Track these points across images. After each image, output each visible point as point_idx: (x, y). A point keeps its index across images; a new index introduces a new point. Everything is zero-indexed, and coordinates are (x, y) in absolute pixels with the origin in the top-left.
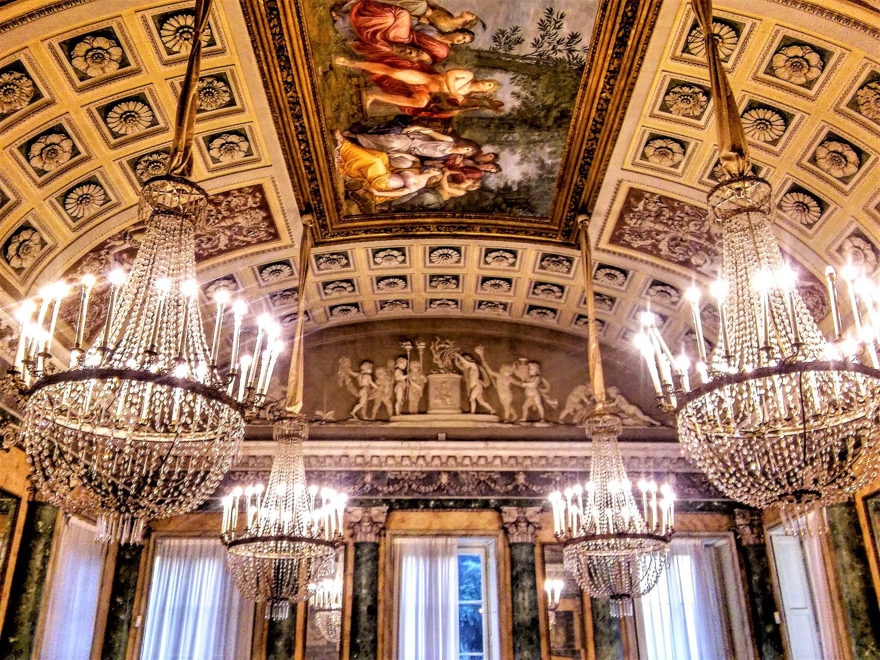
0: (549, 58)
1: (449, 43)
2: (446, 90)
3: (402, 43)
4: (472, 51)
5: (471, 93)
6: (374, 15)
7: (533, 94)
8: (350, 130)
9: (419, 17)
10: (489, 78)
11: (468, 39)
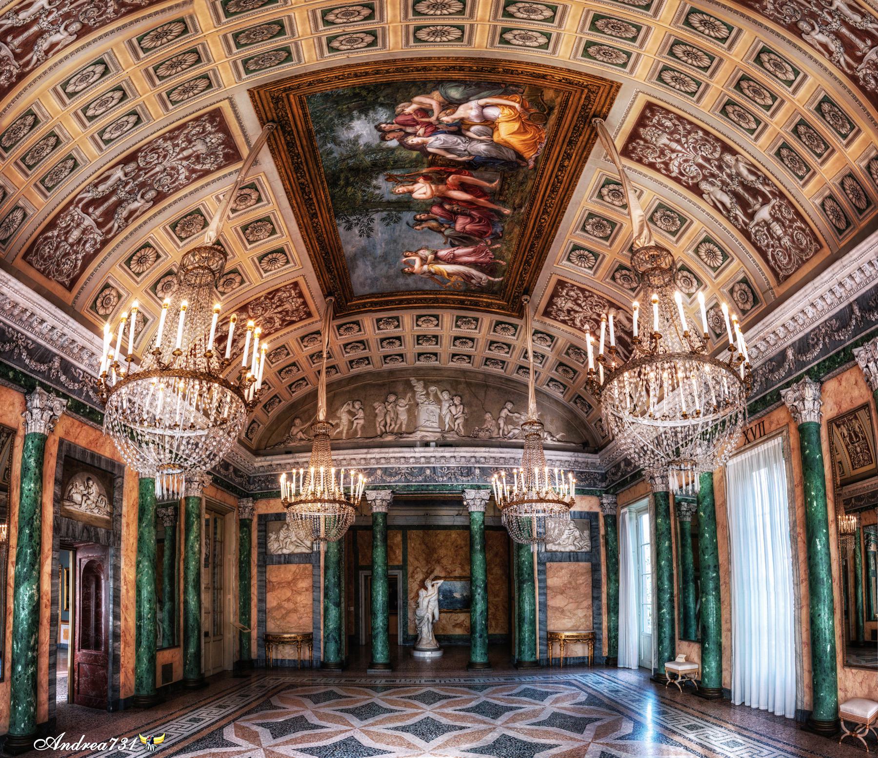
6: (477, 231)
8: (519, 166)
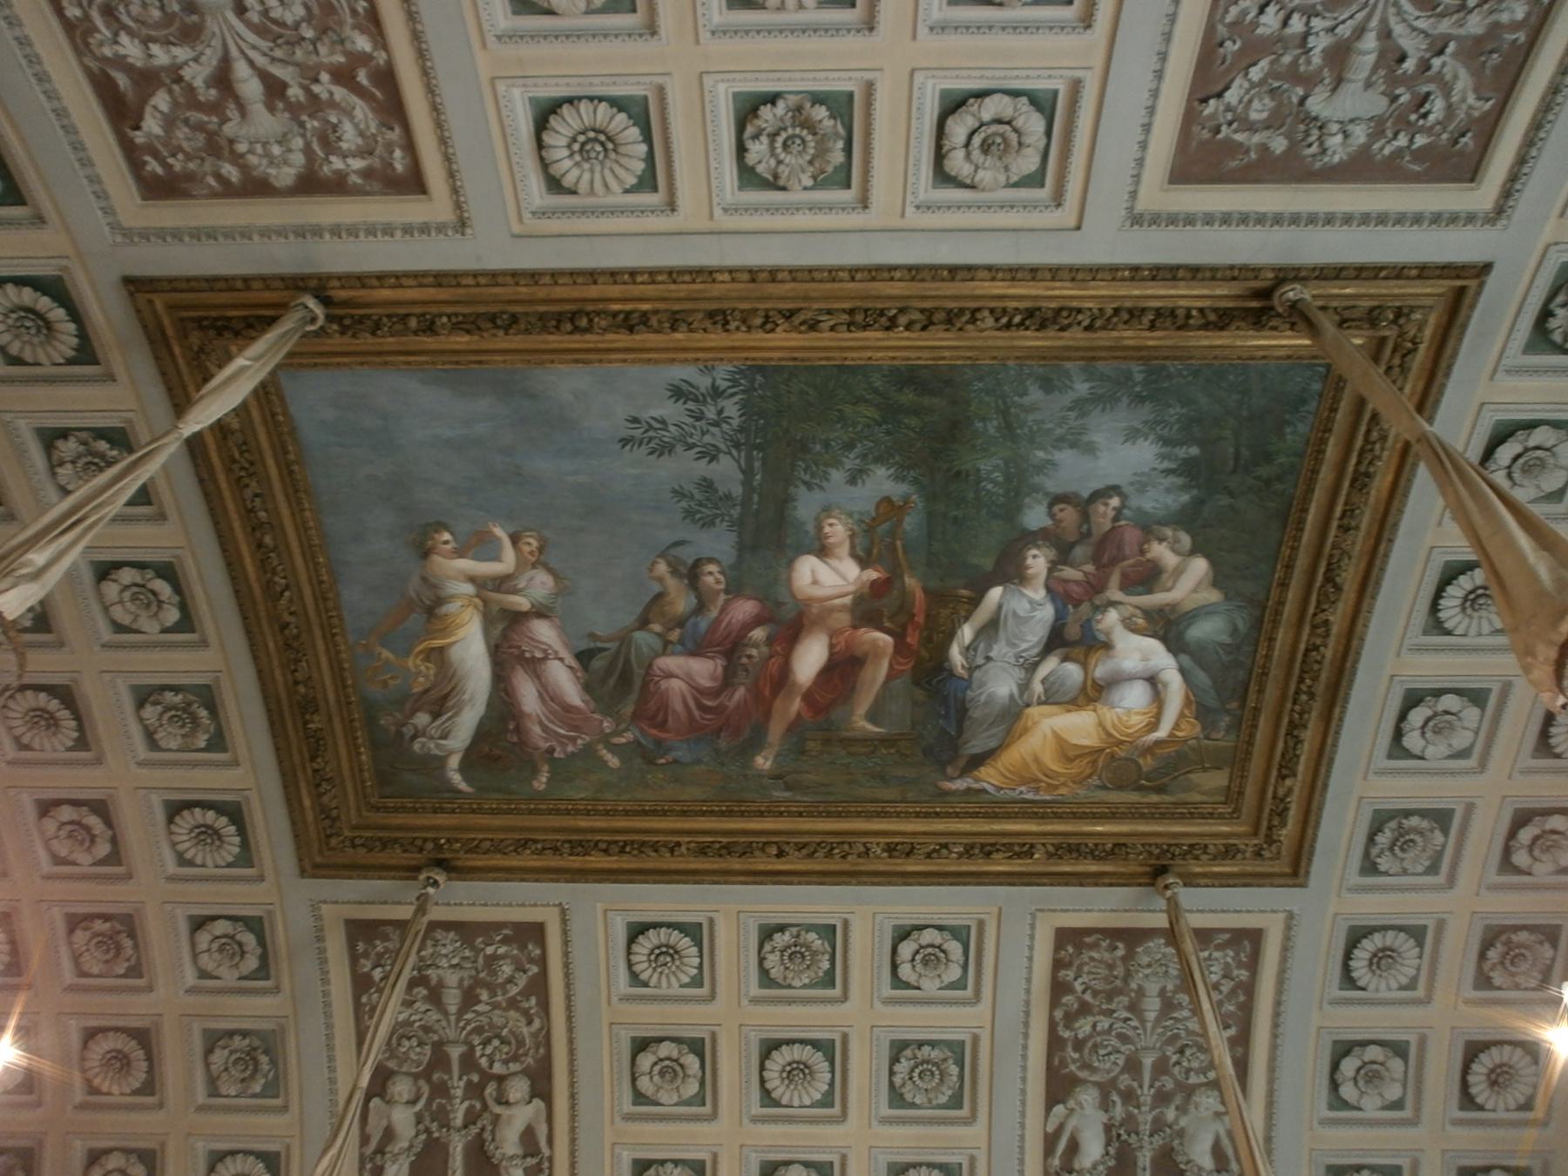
0: (741, 430)
1: (722, 597)
2: (848, 600)
3: (726, 669)
5: (854, 555)
6: (664, 706)
7: (850, 446)
8: (942, 765)
9: (667, 643)
10: (810, 528)
11: (712, 568)
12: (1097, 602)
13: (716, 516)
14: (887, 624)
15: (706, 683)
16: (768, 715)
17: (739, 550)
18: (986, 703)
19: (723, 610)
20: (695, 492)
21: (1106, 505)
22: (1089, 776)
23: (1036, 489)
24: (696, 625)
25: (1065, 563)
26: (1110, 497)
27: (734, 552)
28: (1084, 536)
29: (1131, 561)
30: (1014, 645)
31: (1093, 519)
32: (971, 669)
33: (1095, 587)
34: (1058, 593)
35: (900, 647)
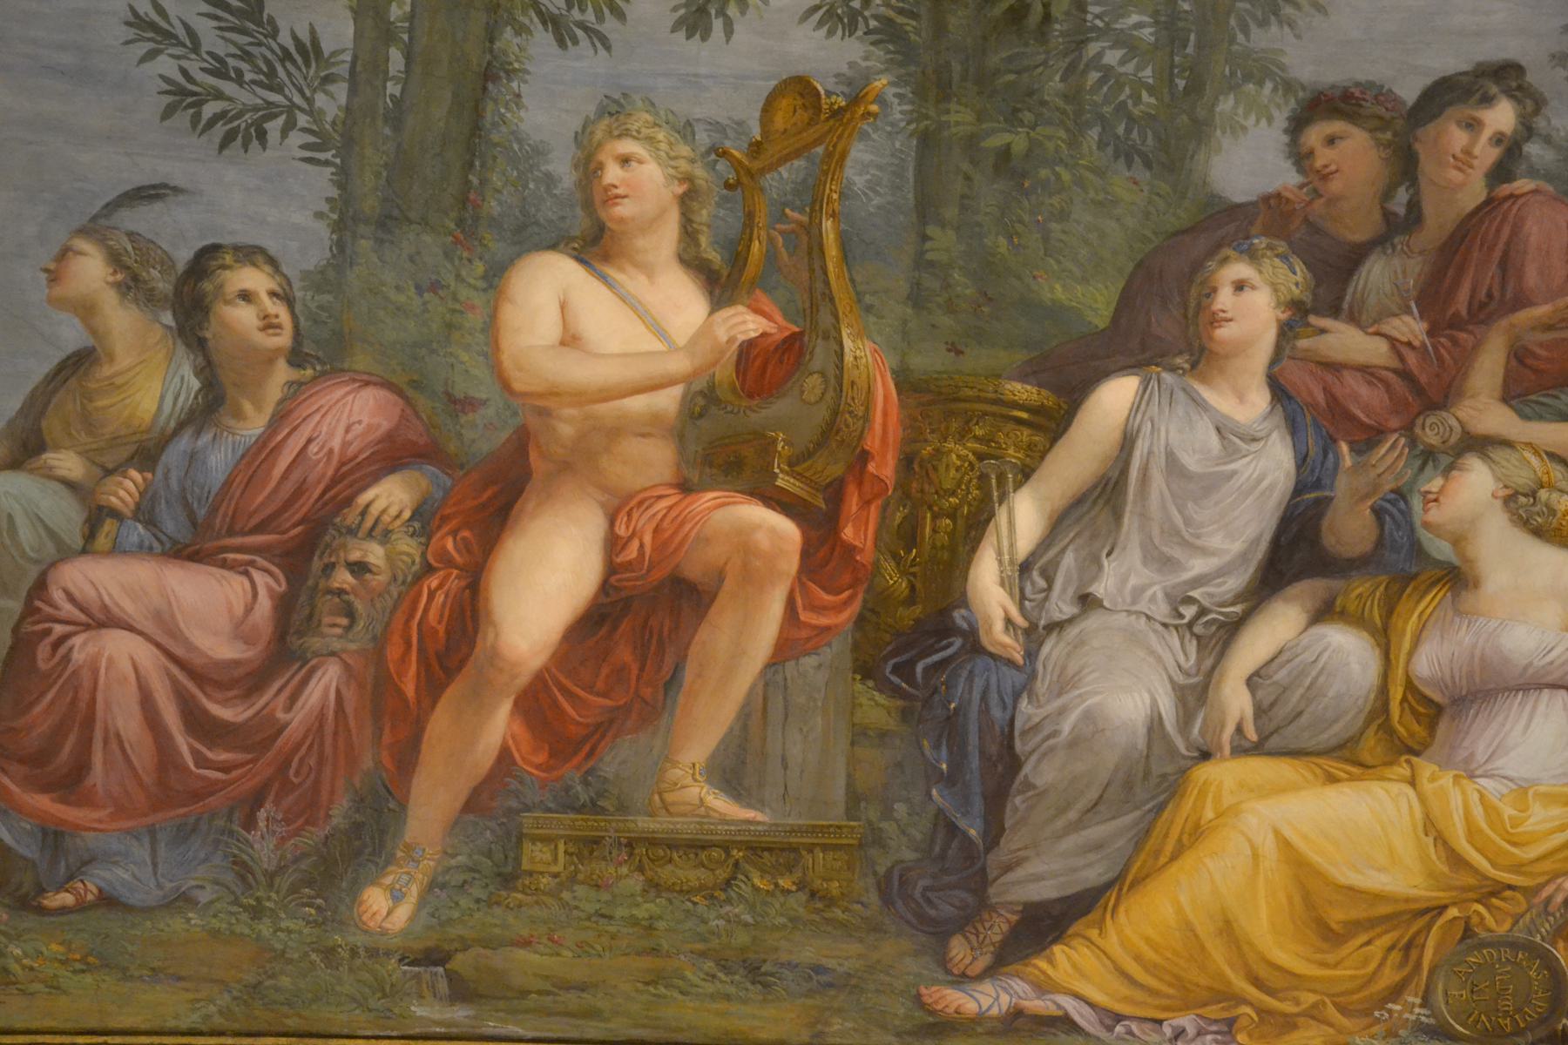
1: (282, 373)
2: (668, 401)
3: (284, 606)
4: (341, 251)
5: (692, 262)
6: (82, 716)
8: (939, 932)
9: (97, 516)
11: (255, 279)
12: (1431, 437)
13: (270, 111)
14: (783, 481)
15: (219, 647)
16: (407, 757)
17: (339, 227)
18: (1073, 744)
19: (280, 417)
20: (206, 29)
21: (1473, 126)
22: (1396, 992)
23: (1260, 69)
24: (192, 457)
25: (1335, 311)
26: (1487, 101)
27: (323, 231)
28: (1399, 226)
29: (1541, 311)
30: (1166, 563)
31: (1427, 166)
32: (1034, 634)
33: (1425, 389)
34: (1312, 408)
35: (823, 555)
